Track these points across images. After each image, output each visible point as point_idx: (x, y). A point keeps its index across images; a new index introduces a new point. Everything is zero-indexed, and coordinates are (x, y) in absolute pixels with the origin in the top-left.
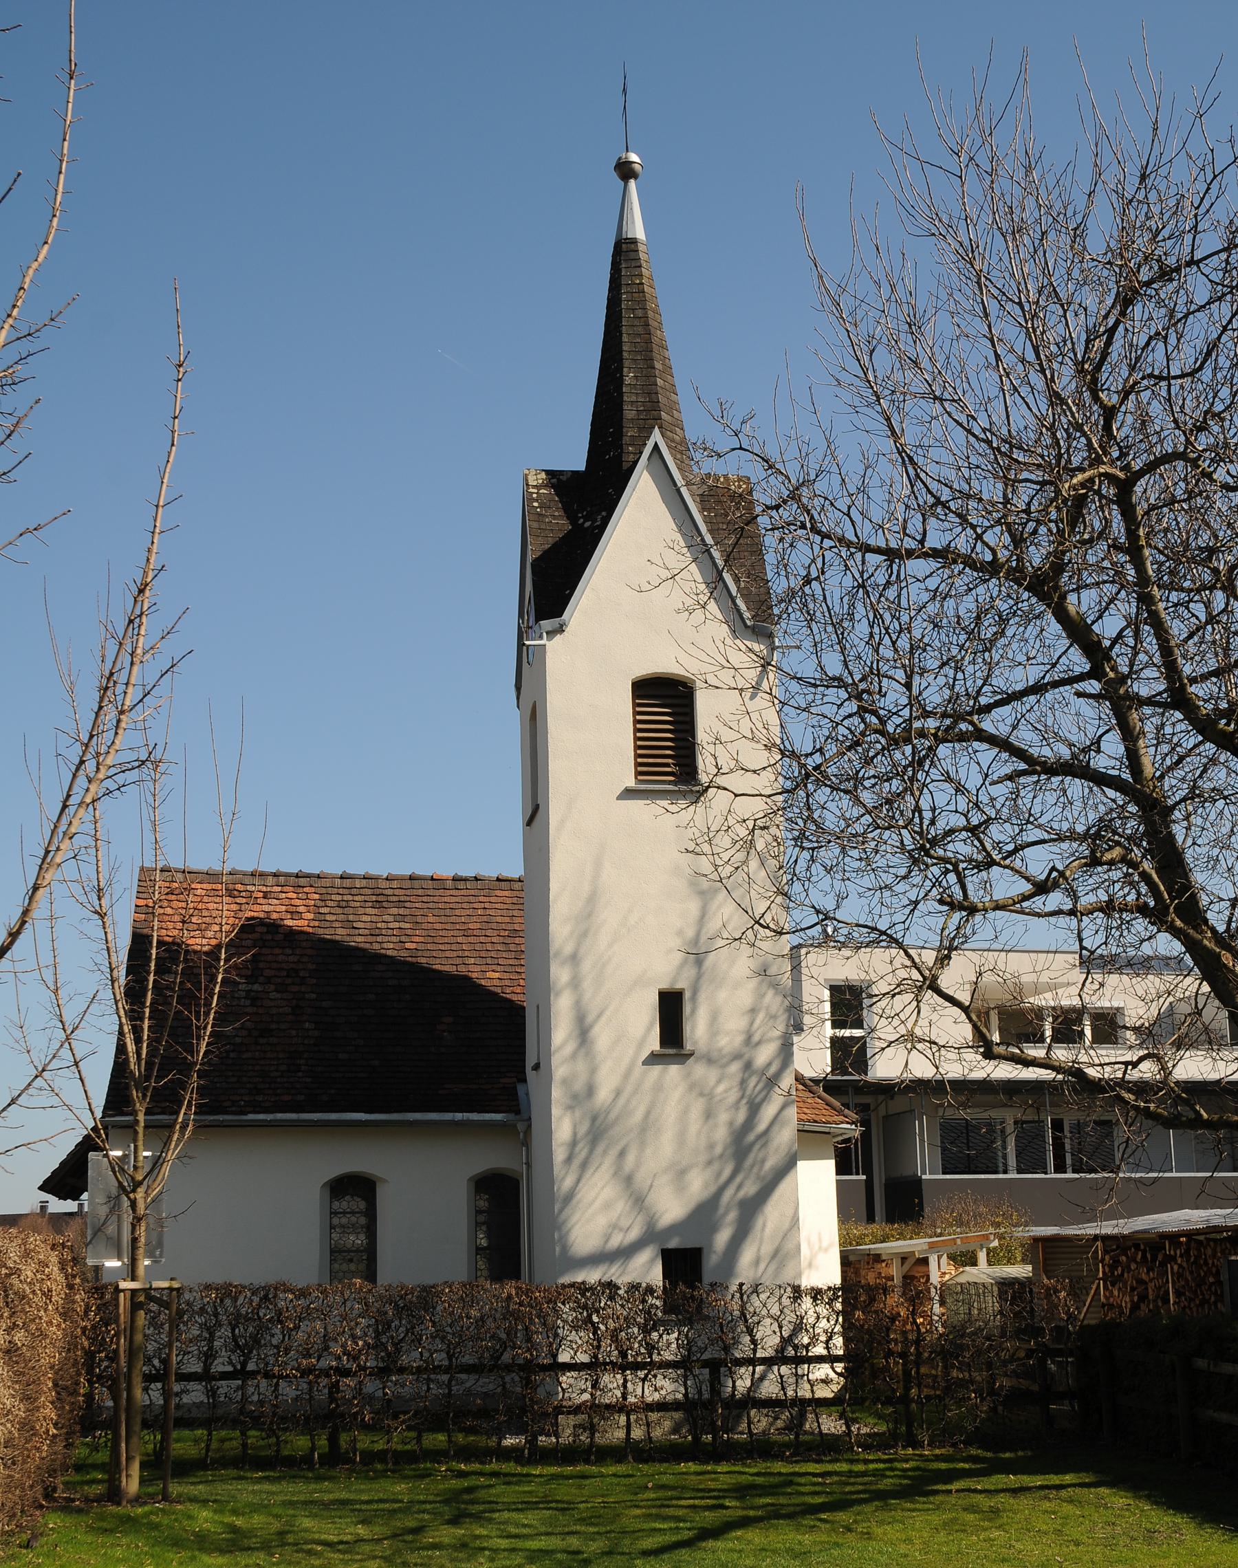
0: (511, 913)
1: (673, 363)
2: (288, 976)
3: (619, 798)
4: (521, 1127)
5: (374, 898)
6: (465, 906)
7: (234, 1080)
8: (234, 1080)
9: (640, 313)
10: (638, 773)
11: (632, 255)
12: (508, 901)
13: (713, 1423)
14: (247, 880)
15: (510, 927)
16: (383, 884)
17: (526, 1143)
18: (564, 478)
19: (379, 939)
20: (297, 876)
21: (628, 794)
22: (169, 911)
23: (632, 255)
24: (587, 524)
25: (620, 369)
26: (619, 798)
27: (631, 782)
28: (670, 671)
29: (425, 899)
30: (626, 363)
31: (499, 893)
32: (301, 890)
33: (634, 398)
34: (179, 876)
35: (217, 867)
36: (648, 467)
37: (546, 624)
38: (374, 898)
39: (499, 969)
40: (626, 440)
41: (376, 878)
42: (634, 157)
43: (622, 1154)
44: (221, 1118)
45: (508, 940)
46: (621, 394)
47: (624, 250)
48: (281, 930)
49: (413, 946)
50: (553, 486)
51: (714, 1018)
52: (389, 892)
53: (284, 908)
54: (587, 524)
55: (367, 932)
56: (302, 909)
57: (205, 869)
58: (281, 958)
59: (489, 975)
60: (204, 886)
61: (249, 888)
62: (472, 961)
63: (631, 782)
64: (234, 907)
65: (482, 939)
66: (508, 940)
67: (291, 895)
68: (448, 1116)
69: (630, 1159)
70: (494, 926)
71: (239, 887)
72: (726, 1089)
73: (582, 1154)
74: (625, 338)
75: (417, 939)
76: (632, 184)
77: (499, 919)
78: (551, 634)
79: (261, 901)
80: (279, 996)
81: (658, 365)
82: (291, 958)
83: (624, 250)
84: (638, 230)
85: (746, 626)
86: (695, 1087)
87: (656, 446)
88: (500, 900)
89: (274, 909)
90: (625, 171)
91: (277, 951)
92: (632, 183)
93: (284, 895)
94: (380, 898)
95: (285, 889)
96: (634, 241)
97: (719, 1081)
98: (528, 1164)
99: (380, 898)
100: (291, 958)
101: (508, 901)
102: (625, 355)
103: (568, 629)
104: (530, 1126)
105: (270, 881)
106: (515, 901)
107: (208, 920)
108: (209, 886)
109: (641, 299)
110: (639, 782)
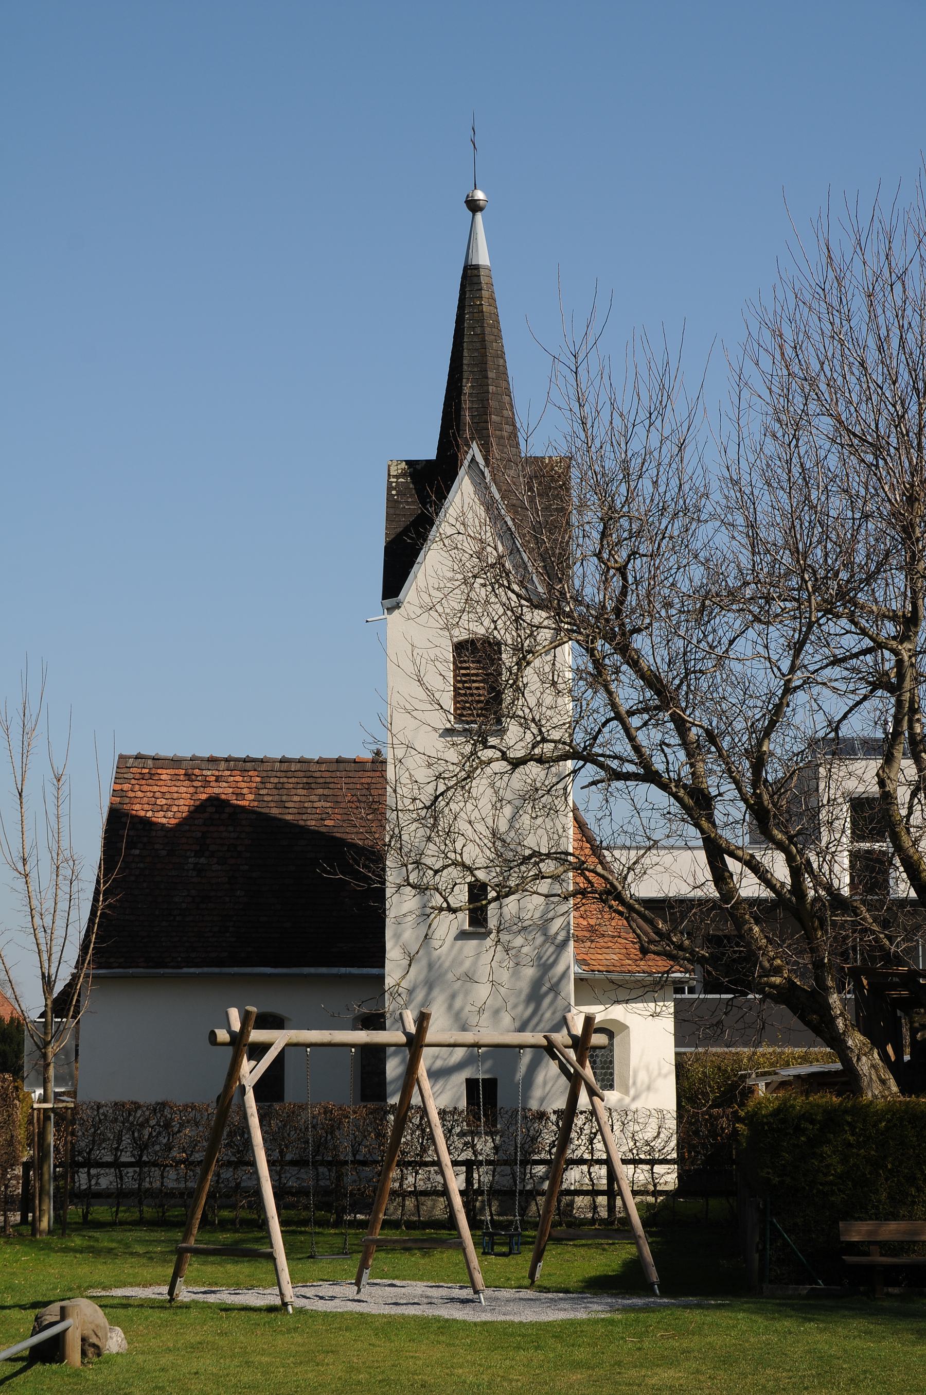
5: (305, 780)
9: (478, 331)
16: (314, 767)
18: (419, 467)
19: (304, 817)
22: (140, 794)
30: (465, 375)
34: (150, 762)
38: (305, 780)
52: (318, 774)
53: (231, 790)
55: (295, 811)
56: (245, 791)
60: (168, 771)
61: (205, 772)
64: (191, 790)
71: (197, 772)
74: (465, 353)
81: (491, 375)
87: (473, 459)
89: (223, 790)
91: (222, 828)
94: (310, 780)
99: (310, 780)
102: (465, 367)
105: (223, 765)
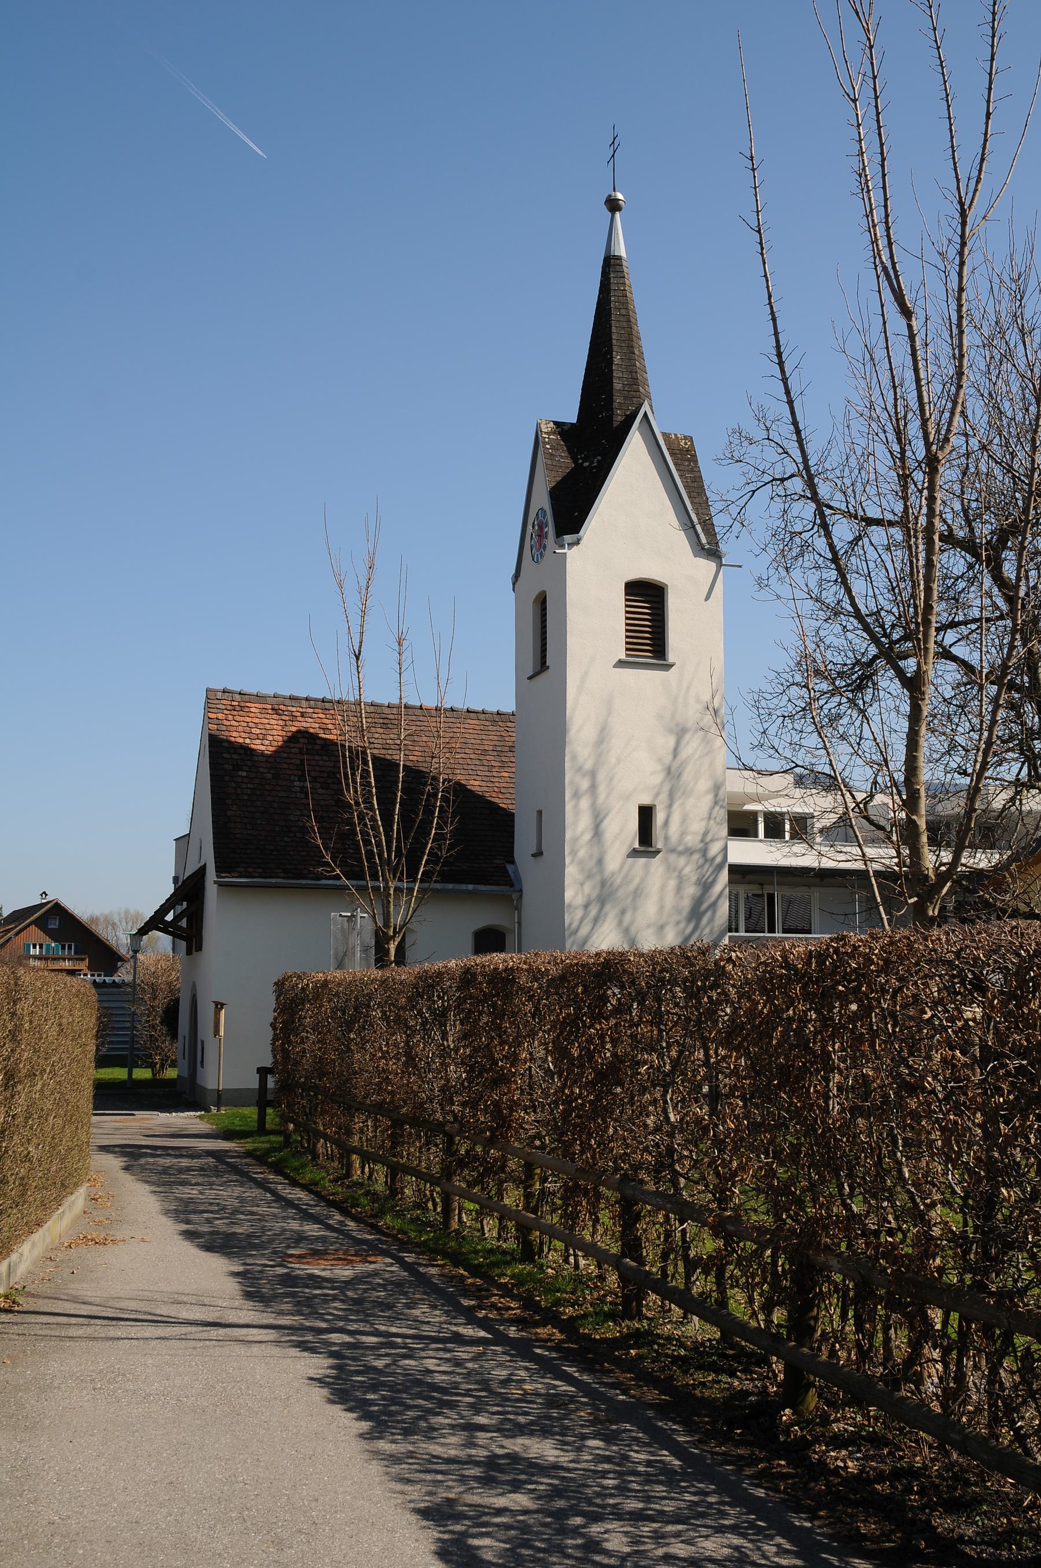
0: (480, 737)
1: (644, 350)
2: (328, 777)
3: (615, 666)
4: (515, 896)
5: (381, 721)
6: (471, 731)
7: (304, 853)
8: (304, 853)
9: (623, 312)
10: (627, 649)
11: (618, 268)
12: (478, 727)
13: (983, 962)
14: (288, 702)
15: (481, 747)
16: (387, 711)
17: (518, 908)
18: (566, 428)
19: (390, 752)
20: (323, 701)
21: (621, 664)
22: (234, 723)
23: (618, 268)
24: (586, 464)
25: (610, 352)
26: (615, 666)
27: (622, 656)
28: (651, 577)
29: (418, 723)
30: (615, 348)
31: (469, 721)
32: (327, 712)
33: (620, 375)
34: (237, 696)
35: (396, 701)
36: (639, 429)
37: (568, 538)
38: (381, 721)
39: (478, 778)
40: (615, 405)
41: (381, 706)
42: (620, 196)
43: (623, 912)
44: (304, 882)
45: (482, 757)
46: (611, 371)
47: (611, 265)
48: (318, 742)
49: (415, 758)
50: (559, 434)
51: (684, 820)
52: (392, 717)
53: (317, 725)
54: (586, 464)
55: (380, 746)
56: (330, 726)
57: (255, 692)
58: (321, 763)
59: (472, 782)
60: (257, 705)
61: (290, 708)
62: (458, 771)
63: (622, 656)
64: (281, 723)
65: (463, 755)
66: (482, 757)
67: (321, 715)
68: (463, 887)
69: (628, 918)
70: (470, 746)
71: (282, 707)
72: (689, 869)
73: (593, 911)
74: (614, 330)
75: (416, 753)
76: (618, 215)
77: (473, 741)
78: (571, 545)
79: (300, 719)
80: (324, 791)
81: (636, 352)
82: (328, 764)
83: (611, 265)
84: (621, 250)
85: (703, 549)
86: (670, 868)
87: (645, 414)
88: (471, 727)
89: (310, 725)
90: (613, 205)
91: (318, 758)
92: (618, 214)
93: (315, 716)
94: (386, 721)
95: (316, 710)
96: (619, 258)
97: (686, 865)
98: (519, 923)
99: (386, 721)
100: (328, 764)
101: (478, 727)
102: (614, 342)
103: (581, 542)
104: (521, 896)
105: (304, 703)
106: (482, 727)
107: (263, 731)
108: (261, 706)
109: (625, 302)
110: (627, 655)
